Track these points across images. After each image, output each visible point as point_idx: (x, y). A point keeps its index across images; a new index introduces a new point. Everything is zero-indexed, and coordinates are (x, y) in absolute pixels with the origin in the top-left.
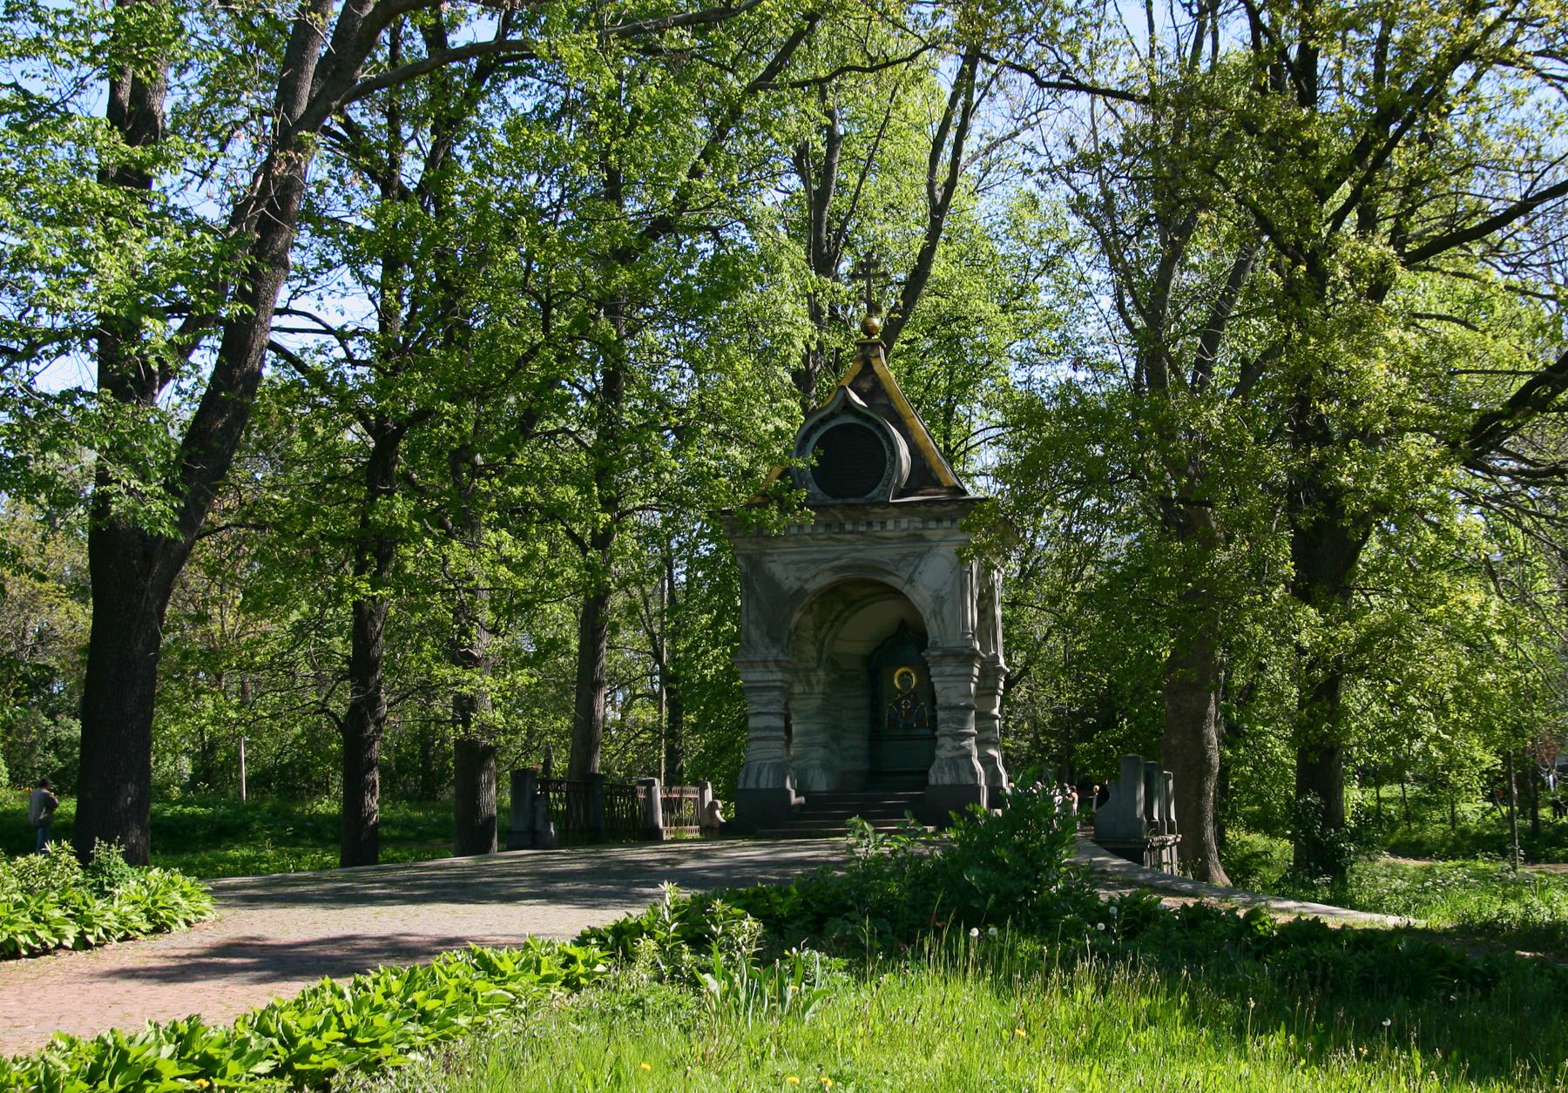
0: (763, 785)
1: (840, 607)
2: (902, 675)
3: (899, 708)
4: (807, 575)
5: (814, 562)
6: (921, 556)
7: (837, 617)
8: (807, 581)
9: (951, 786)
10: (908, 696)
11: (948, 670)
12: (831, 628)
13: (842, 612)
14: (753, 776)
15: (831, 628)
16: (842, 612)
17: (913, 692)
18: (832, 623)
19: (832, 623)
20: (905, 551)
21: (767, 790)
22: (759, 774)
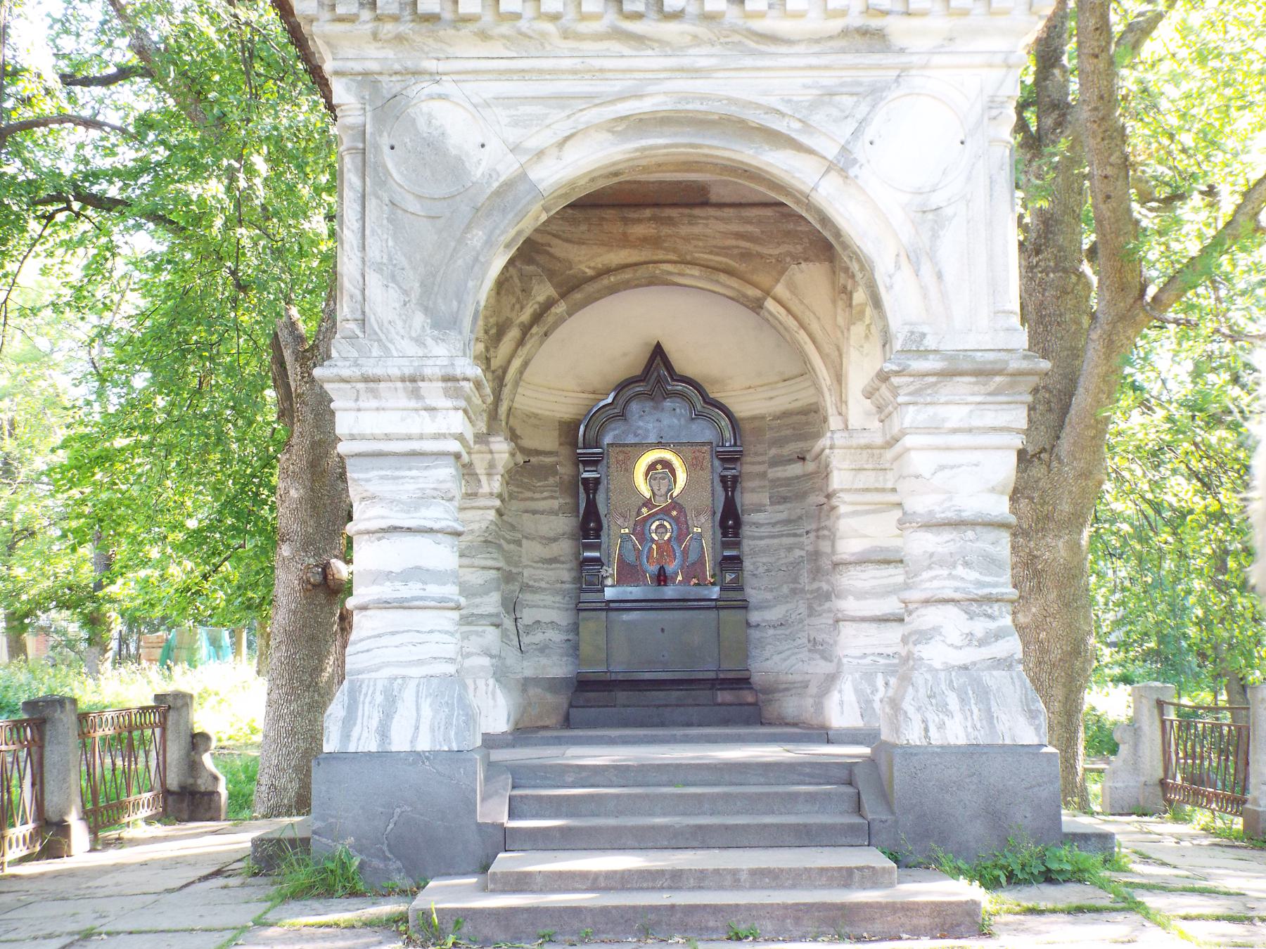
0: (400, 742)
1: (543, 291)
2: (652, 467)
3: (643, 537)
4: (536, 141)
5: (560, 100)
6: (875, 93)
7: (537, 318)
8: (540, 154)
9: (972, 752)
10: (666, 511)
11: (955, 415)
12: (521, 342)
13: (548, 305)
14: (369, 716)
15: (521, 342)
16: (548, 305)
17: (675, 505)
18: (526, 330)
19: (526, 330)
20: (828, 79)
21: (417, 757)
22: (391, 701)
